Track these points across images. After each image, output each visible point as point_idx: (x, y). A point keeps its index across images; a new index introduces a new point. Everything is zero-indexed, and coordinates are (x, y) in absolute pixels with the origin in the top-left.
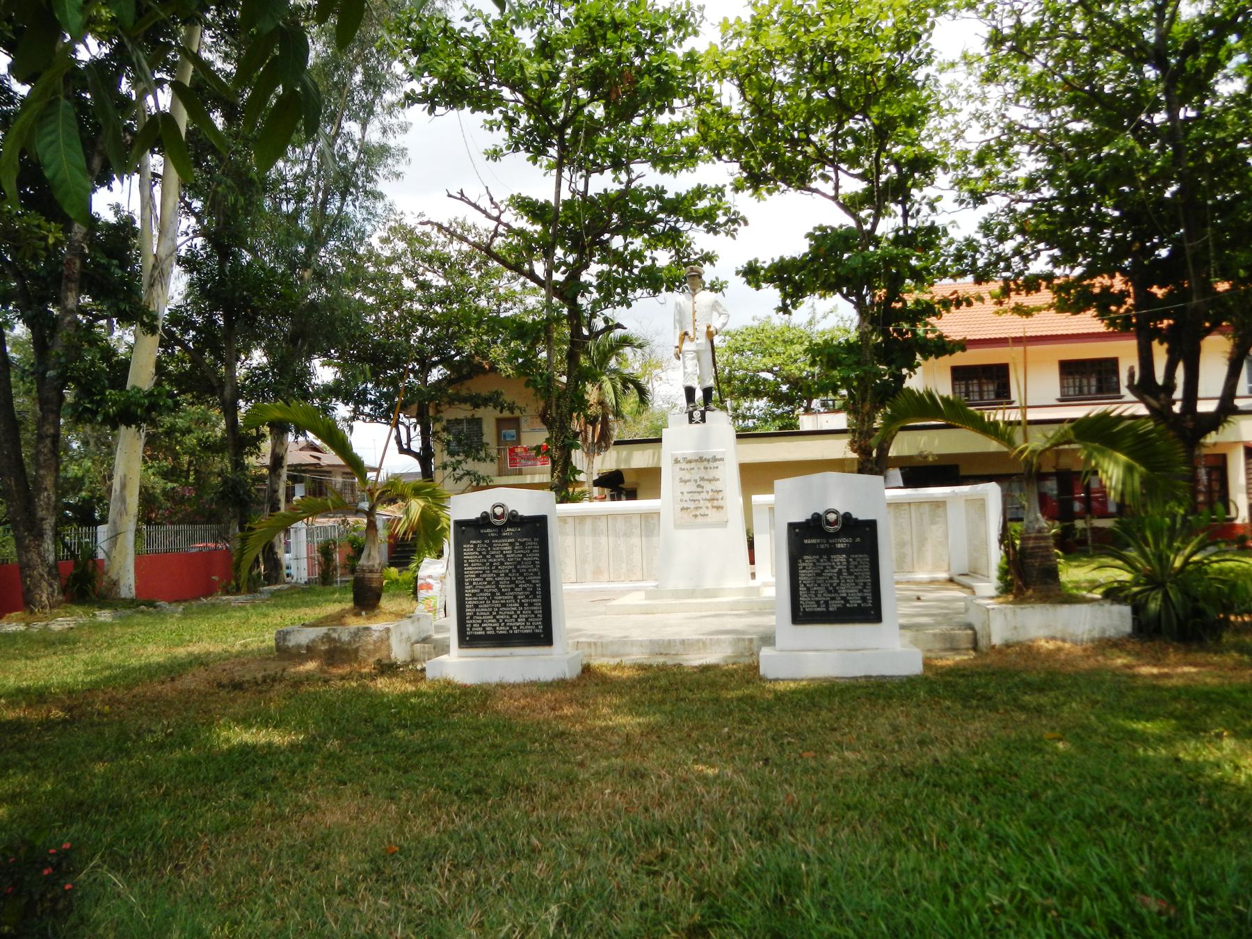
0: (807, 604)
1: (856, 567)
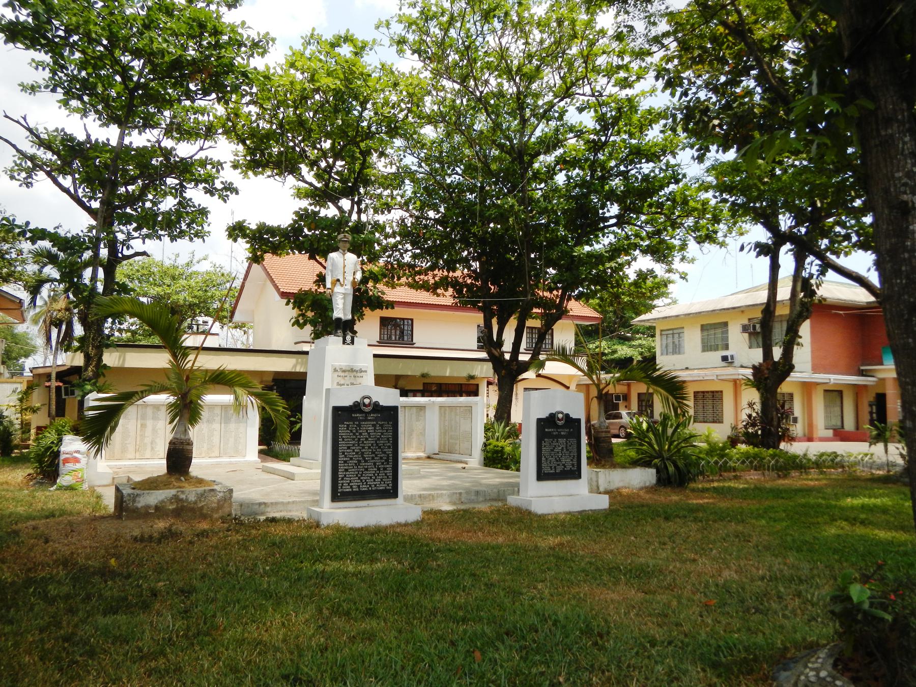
0: (546, 470)
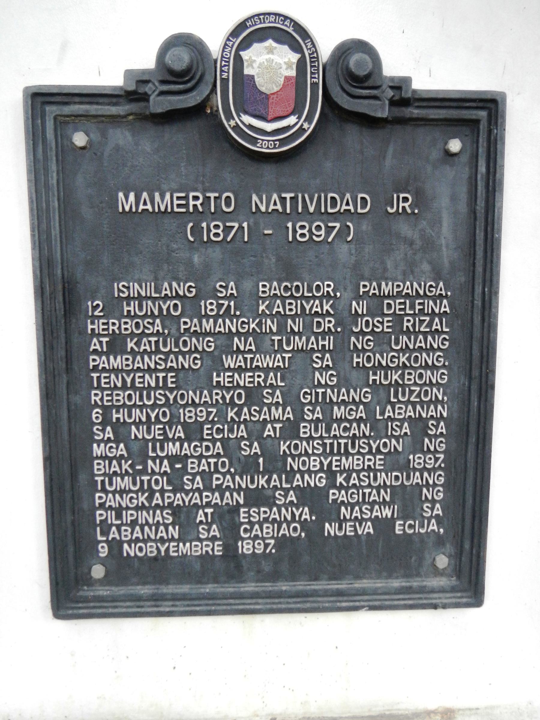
1: (382, 340)
